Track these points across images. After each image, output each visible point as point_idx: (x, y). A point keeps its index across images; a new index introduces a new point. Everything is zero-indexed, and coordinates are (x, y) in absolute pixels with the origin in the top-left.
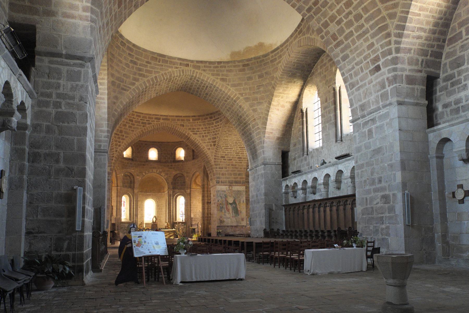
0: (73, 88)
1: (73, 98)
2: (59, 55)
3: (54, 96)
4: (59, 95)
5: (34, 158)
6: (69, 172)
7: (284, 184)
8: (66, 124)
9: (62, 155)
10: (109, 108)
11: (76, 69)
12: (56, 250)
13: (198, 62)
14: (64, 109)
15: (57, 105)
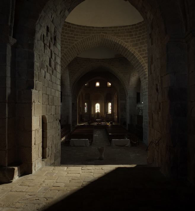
7: (137, 106)
10: (70, 81)
13: (102, 59)
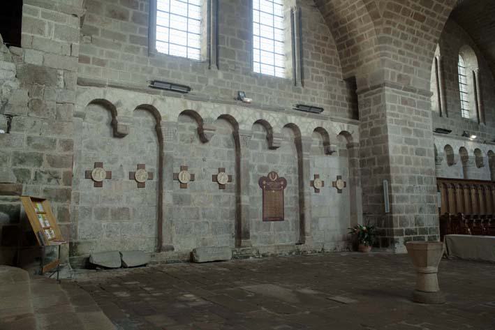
0: (378, 110)
1: (378, 117)
2: (368, 90)
3: (369, 119)
4: (372, 117)
5: (362, 163)
6: (380, 170)
8: (376, 136)
9: (376, 159)
11: (377, 95)
12: (378, 226)
14: (375, 126)
15: (371, 124)
